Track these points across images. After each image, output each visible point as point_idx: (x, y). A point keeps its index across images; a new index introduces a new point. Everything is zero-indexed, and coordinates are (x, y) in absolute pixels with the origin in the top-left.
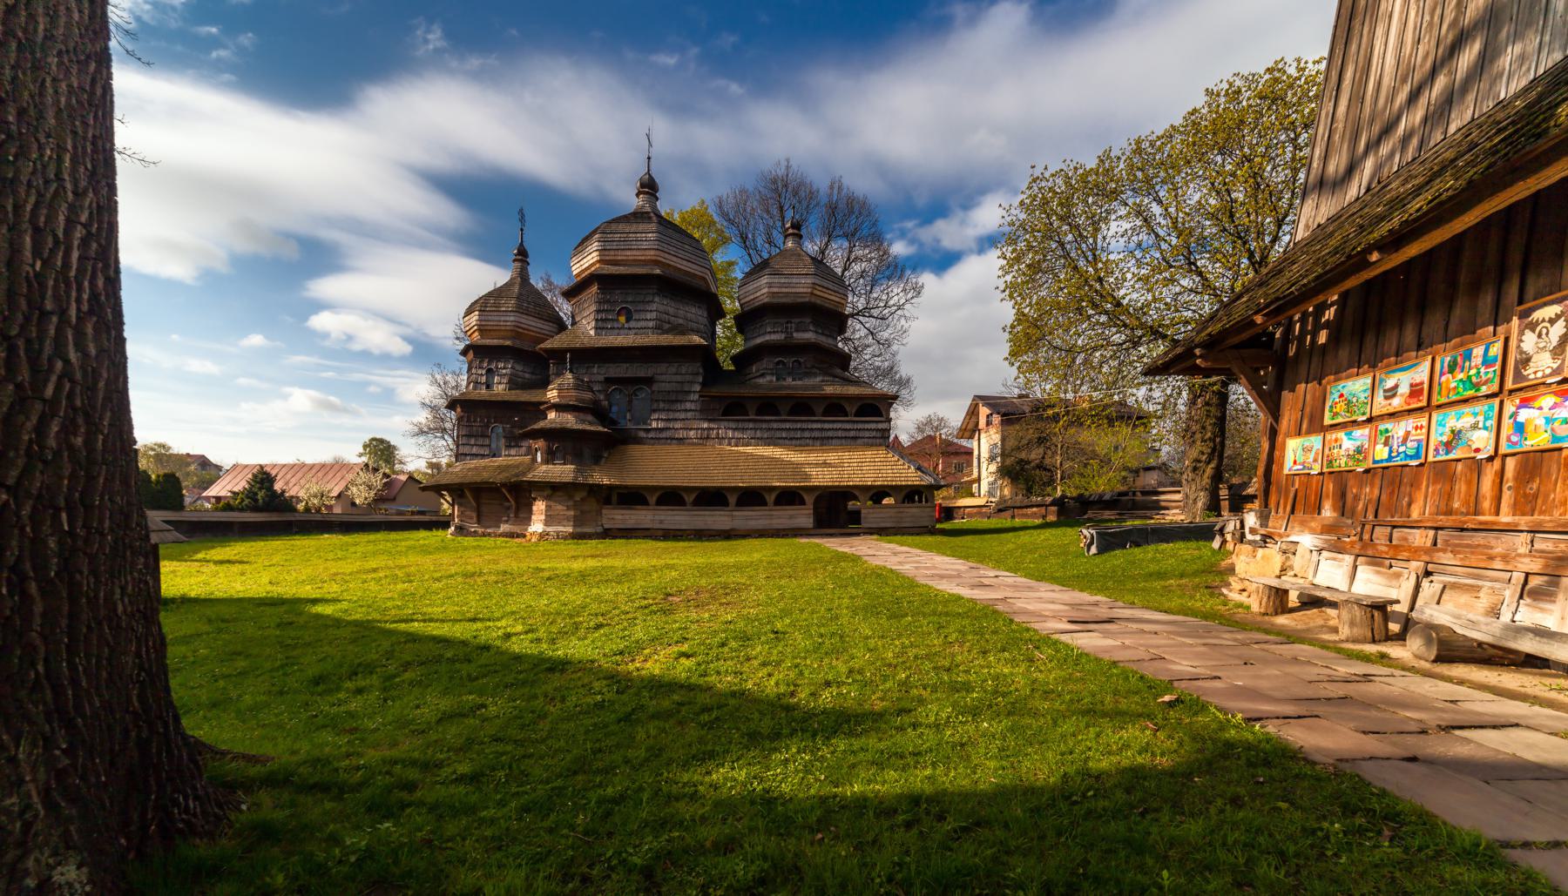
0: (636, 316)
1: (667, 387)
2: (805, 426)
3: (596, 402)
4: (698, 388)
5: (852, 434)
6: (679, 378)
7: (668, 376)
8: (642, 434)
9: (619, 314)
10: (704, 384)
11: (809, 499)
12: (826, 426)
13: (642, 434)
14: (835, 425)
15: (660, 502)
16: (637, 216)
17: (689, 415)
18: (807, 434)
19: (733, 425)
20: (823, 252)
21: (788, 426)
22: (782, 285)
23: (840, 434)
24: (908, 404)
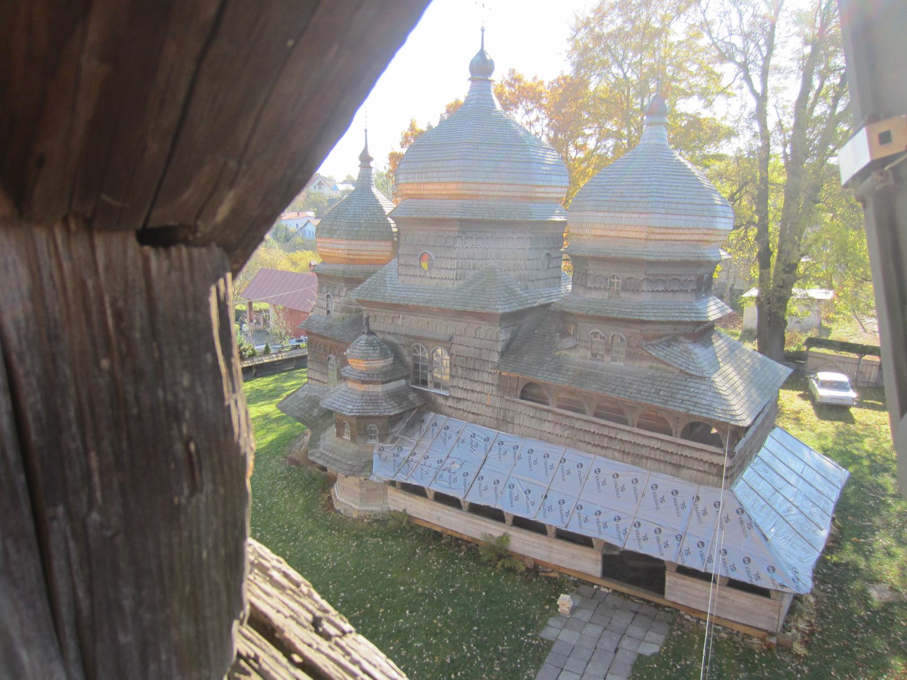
4: (496, 358)
5: (675, 459)
13: (441, 400)
17: (486, 388)
18: (616, 445)
21: (592, 428)
23: (658, 455)
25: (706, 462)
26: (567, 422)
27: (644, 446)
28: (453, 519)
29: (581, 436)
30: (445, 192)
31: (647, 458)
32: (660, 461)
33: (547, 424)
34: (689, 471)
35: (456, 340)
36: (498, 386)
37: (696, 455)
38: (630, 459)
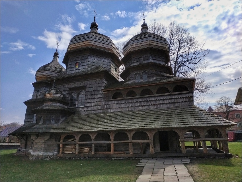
2: (148, 99)
3: (64, 97)
4: (103, 88)
5: (173, 101)
6: (96, 85)
7: (91, 84)
8: (81, 109)
9: (76, 65)
12: (159, 98)
17: (99, 100)
18: (150, 103)
19: (116, 102)
21: (140, 100)
23: (166, 101)
25: (184, 97)
26: (130, 101)
27: (160, 100)
33: (123, 105)
34: (179, 103)
35: (88, 86)
36: (104, 98)
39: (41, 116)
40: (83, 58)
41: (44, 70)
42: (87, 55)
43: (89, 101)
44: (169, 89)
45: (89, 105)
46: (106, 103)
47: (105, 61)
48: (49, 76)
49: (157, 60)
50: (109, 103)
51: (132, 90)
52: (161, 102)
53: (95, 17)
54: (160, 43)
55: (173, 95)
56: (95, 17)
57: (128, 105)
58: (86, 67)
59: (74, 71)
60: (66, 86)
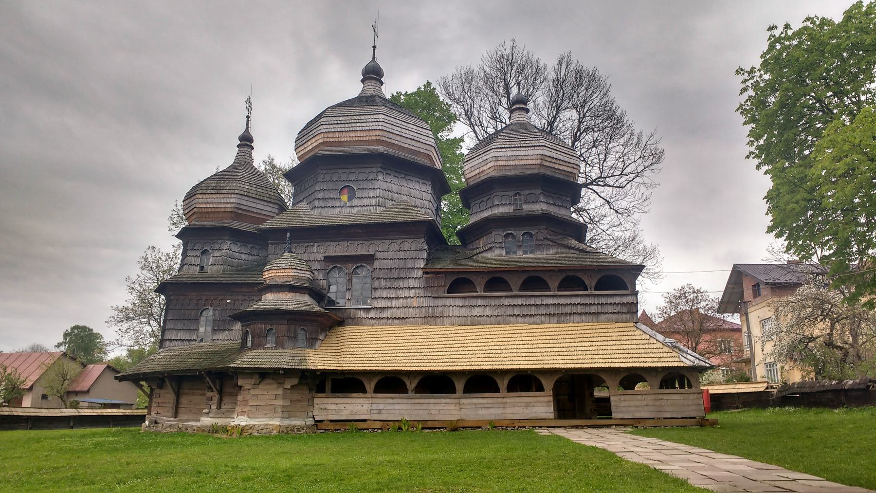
0: (359, 194)
1: (390, 264)
2: (538, 301)
3: (313, 281)
4: (422, 264)
5: (594, 309)
6: (402, 255)
7: (389, 253)
8: (361, 314)
9: (341, 192)
10: (427, 261)
11: (548, 384)
13: (361, 314)
14: (571, 299)
15: (379, 389)
16: (363, 100)
17: (412, 293)
18: (542, 311)
19: (460, 302)
20: (551, 124)
21: (520, 301)
22: (509, 158)
23: (579, 309)
24: (655, 276)
27: (567, 304)
28: (397, 407)
29: (510, 311)
30: (367, 138)
31: (570, 314)
32: (581, 314)
33: (477, 309)
34: (606, 316)
35: (378, 255)
37: (610, 300)
38: (555, 320)
39: (269, 326)
40: (362, 177)
41: (225, 191)
42: (374, 170)
43: (385, 294)
44: (587, 282)
45: (383, 303)
46: (433, 302)
47: (418, 187)
48: (240, 212)
49: (555, 205)
50: (441, 302)
51: (499, 275)
52: (568, 310)
53: (374, 47)
54: (563, 163)
55: (595, 296)
56: (374, 47)
57: (488, 312)
58: (374, 201)
59: (337, 210)
60: (315, 249)
